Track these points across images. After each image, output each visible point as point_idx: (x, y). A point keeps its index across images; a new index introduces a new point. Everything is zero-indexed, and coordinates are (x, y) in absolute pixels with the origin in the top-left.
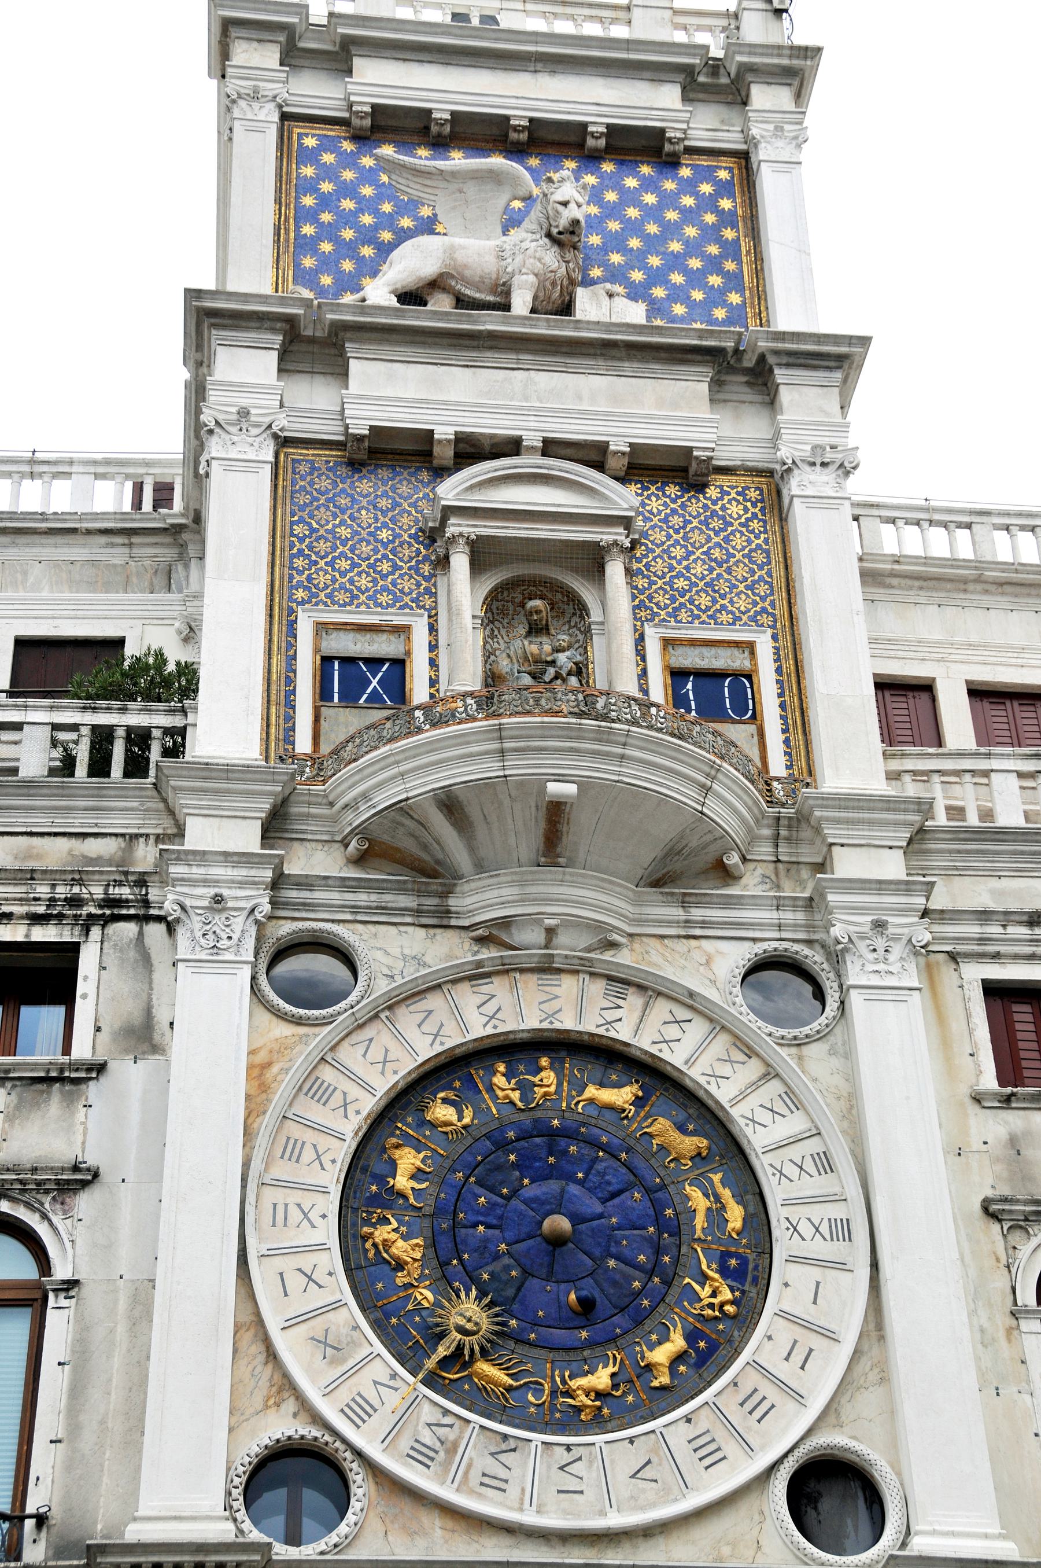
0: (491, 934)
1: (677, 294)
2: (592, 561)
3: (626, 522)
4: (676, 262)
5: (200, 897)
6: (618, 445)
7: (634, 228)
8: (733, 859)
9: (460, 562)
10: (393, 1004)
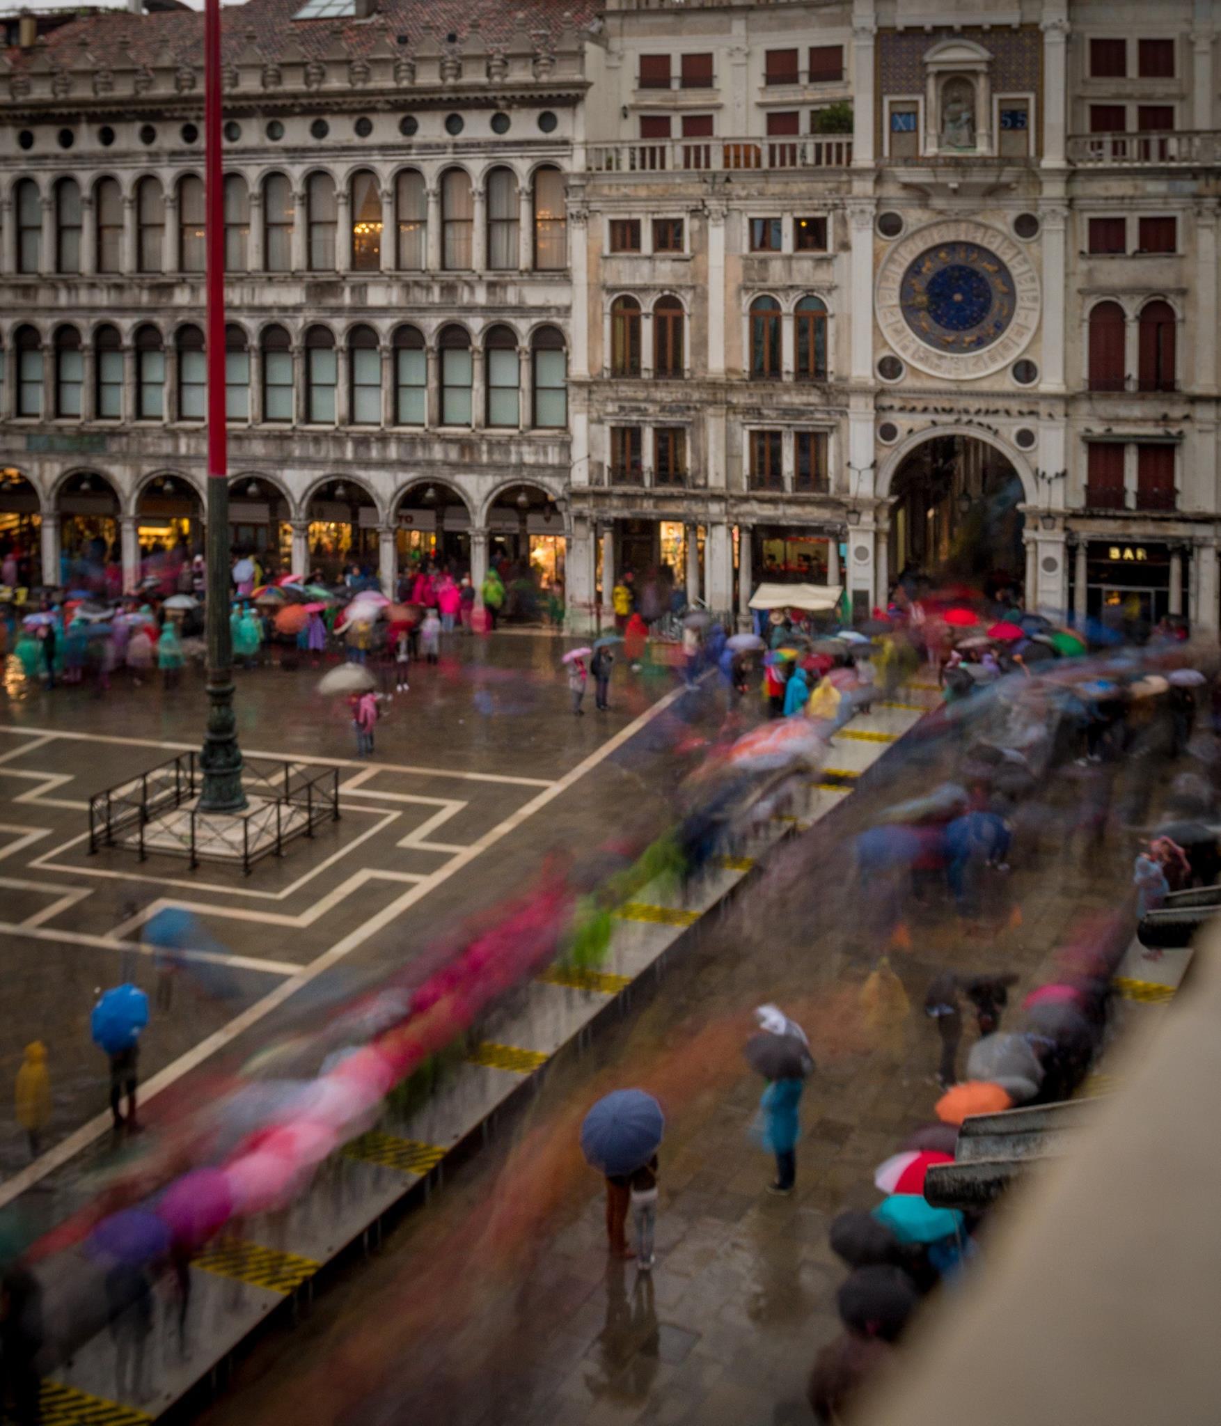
0: (941, 212)
5: (858, 208)
6: (986, 27)
8: (1014, 185)
10: (913, 234)
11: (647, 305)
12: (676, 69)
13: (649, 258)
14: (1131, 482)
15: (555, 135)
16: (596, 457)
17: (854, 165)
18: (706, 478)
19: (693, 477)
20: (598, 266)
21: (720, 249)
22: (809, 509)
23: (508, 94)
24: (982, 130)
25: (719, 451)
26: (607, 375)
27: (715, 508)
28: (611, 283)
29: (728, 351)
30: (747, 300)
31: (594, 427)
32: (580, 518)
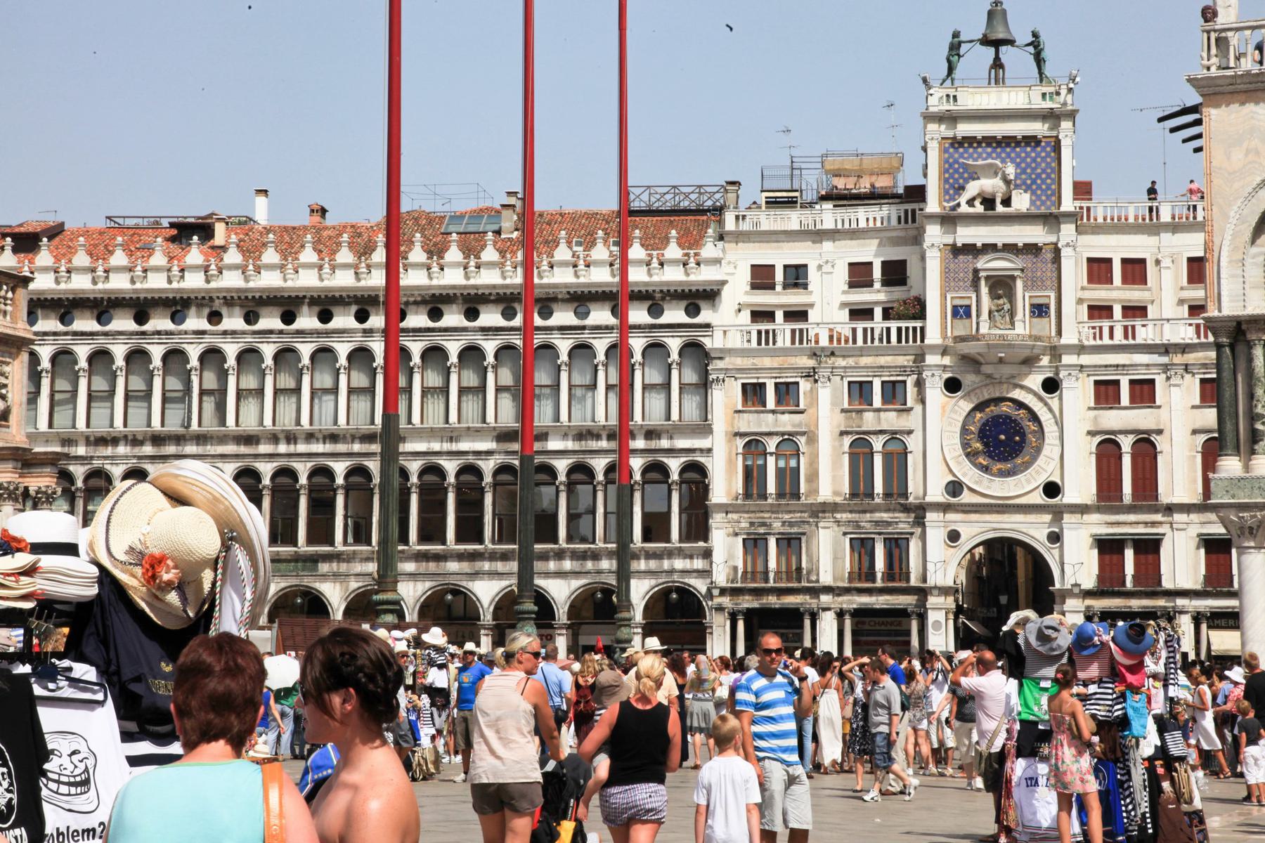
0: (989, 376)
1: (1039, 187)
2: (1013, 278)
3: (1022, 270)
4: (1039, 176)
6: (1020, 245)
7: (1028, 165)
9: (983, 282)
11: (771, 445)
12: (779, 276)
13: (773, 412)
14: (1129, 569)
15: (698, 320)
16: (731, 563)
17: (927, 342)
18: (818, 575)
19: (809, 573)
20: (733, 418)
21: (826, 406)
23: (665, 289)
24: (1019, 316)
25: (828, 554)
27: (825, 599)
28: (742, 430)
29: (834, 478)
30: (847, 440)
31: (731, 539)
32: (720, 609)
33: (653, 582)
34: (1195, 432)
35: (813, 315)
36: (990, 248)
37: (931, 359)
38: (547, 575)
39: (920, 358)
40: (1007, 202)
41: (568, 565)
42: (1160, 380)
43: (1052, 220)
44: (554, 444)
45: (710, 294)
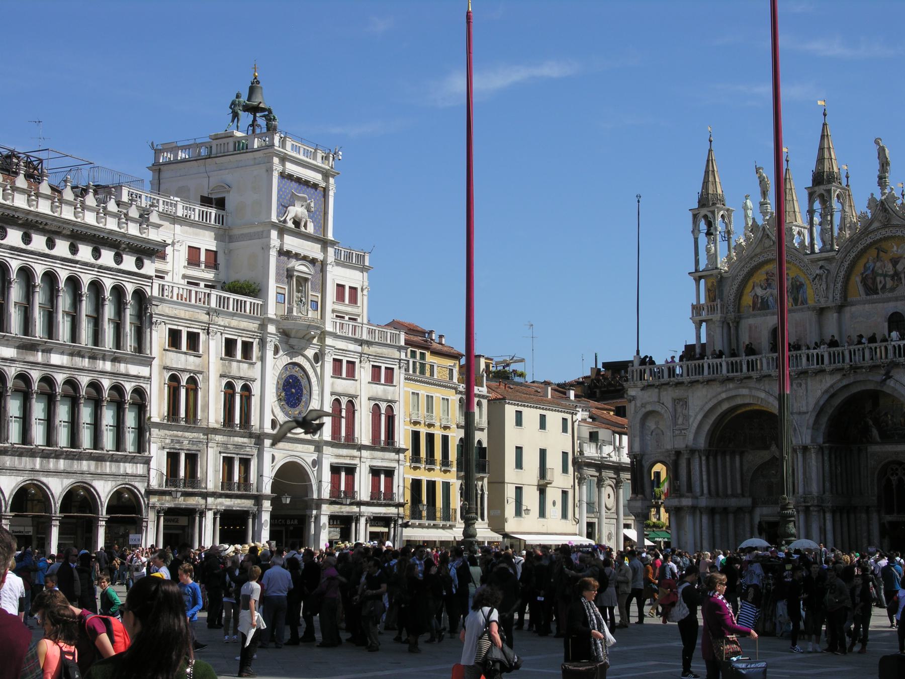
0: (292, 347)
13: (185, 353)
15: (142, 271)
22: (243, 501)
23: (132, 242)
26: (165, 422)
27: (210, 500)
28: (169, 364)
30: (224, 381)
32: (153, 507)
33: (114, 483)
34: (369, 399)
35: (168, 278)
36: (297, 256)
37: (271, 329)
38: (48, 473)
39: (263, 327)
40: (305, 226)
41: (62, 464)
42: (357, 361)
43: (325, 244)
44: (56, 359)
45: (155, 251)
